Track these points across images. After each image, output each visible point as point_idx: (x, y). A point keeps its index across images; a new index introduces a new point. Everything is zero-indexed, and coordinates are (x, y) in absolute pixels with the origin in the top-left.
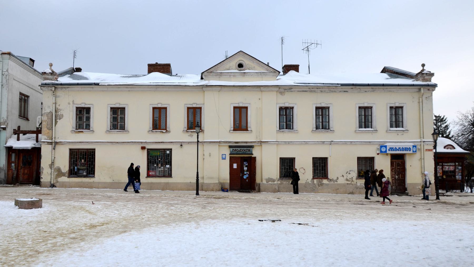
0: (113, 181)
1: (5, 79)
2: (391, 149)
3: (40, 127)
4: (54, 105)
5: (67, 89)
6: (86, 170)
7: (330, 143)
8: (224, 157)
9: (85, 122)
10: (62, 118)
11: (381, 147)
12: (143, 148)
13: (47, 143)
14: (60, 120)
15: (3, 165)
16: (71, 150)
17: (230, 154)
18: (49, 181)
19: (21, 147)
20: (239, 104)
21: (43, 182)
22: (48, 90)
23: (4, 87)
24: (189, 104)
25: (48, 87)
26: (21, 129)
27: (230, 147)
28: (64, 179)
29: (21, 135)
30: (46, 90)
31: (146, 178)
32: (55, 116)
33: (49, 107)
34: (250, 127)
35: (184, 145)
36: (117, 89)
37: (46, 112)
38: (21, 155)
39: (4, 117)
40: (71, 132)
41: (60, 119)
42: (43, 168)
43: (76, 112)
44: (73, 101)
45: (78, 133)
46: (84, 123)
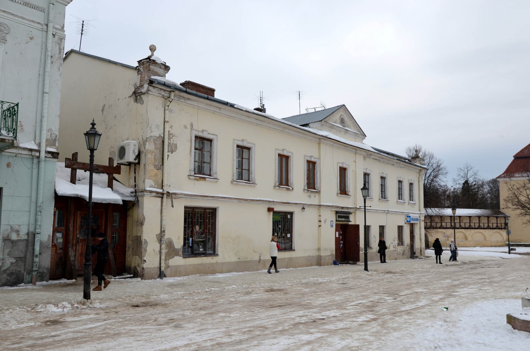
5: (187, 102)
10: (176, 151)
13: (155, 194)
14: (172, 153)
15: (47, 237)
18: (156, 266)
19: (105, 200)
21: (147, 268)
22: (159, 95)
23: (54, 63)
25: (161, 89)
26: (79, 160)
28: (178, 261)
30: (155, 94)
36: (246, 119)
37: (153, 134)
38: (78, 214)
39: (54, 129)
42: (146, 242)
44: (192, 125)
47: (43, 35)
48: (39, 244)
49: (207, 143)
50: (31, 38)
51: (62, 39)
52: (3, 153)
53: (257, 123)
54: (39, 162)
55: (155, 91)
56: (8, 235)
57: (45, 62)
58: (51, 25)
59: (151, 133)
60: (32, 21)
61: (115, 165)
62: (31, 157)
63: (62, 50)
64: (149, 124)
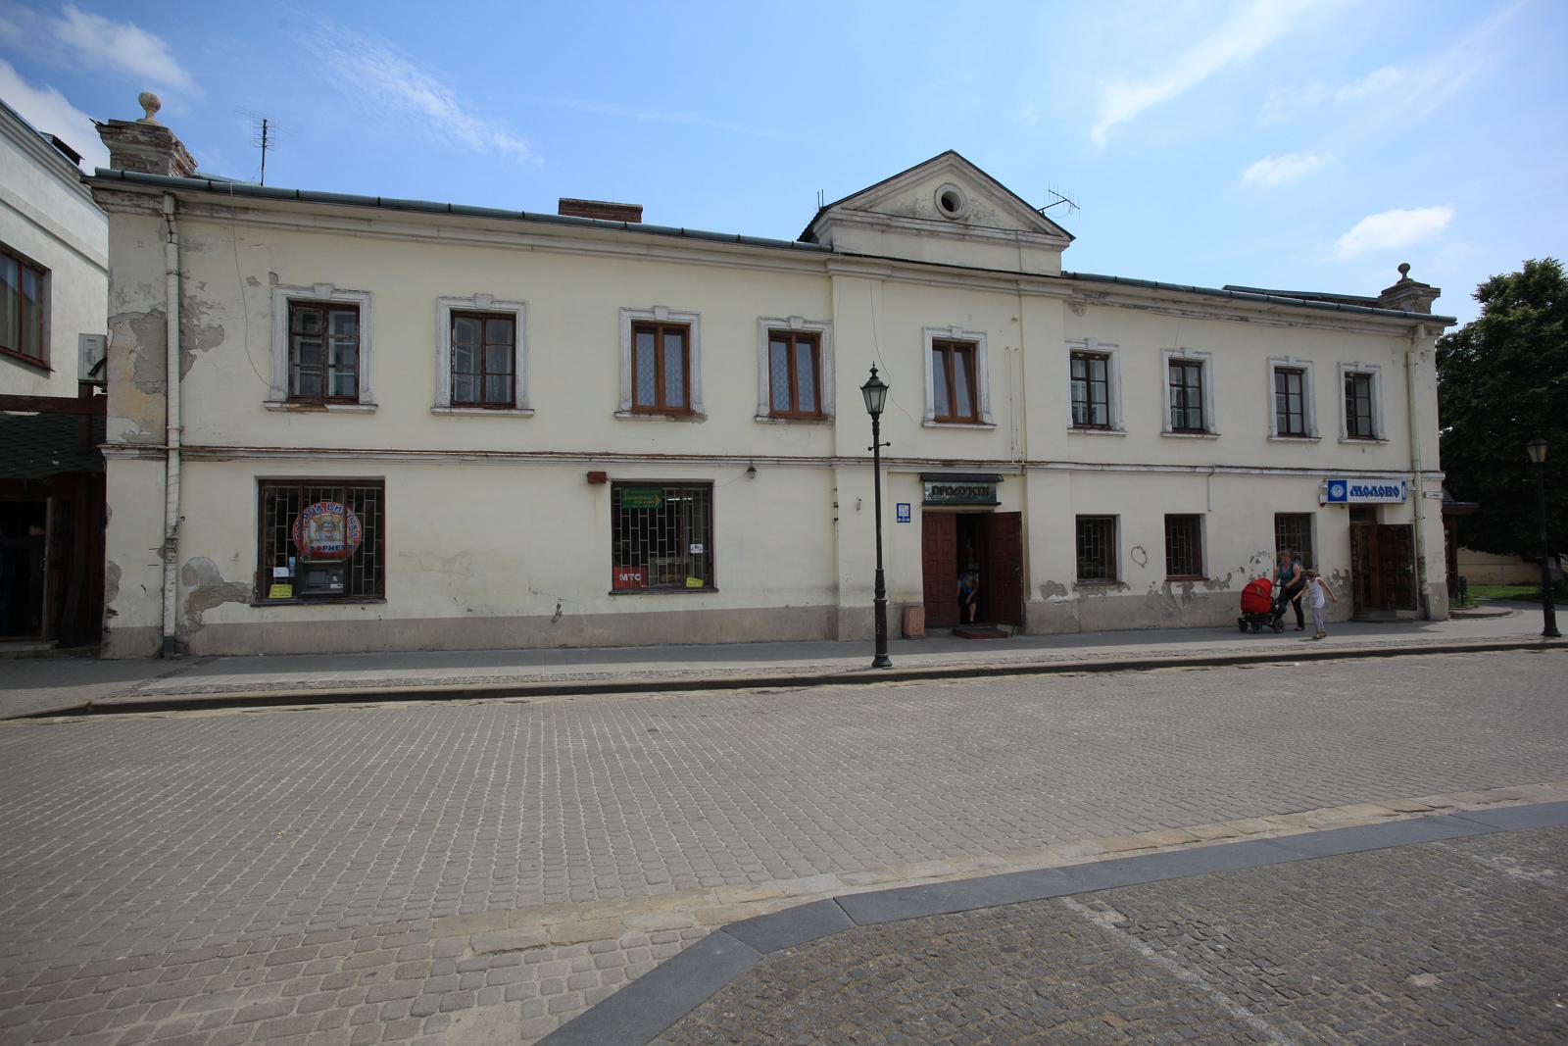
0: (470, 615)
2: (1357, 490)
3: (100, 377)
4: (173, 280)
6: (341, 572)
7: (1210, 470)
8: (903, 512)
9: (333, 366)
11: (1331, 484)
12: (596, 479)
13: (137, 452)
16: (262, 483)
17: (925, 503)
20: (951, 331)
21: (114, 628)
22: (140, 210)
24: (778, 319)
25: (139, 195)
27: (924, 478)
31: (612, 598)
32: (181, 331)
33: (146, 289)
34: (988, 412)
35: (760, 472)
40: (267, 405)
41: (206, 346)
42: (116, 569)
43: (291, 320)
44: (274, 276)
45: (301, 412)
46: (326, 371)
49: (672, 343)
53: (531, 242)
55: (120, 202)
59: (122, 305)
64: (115, 285)
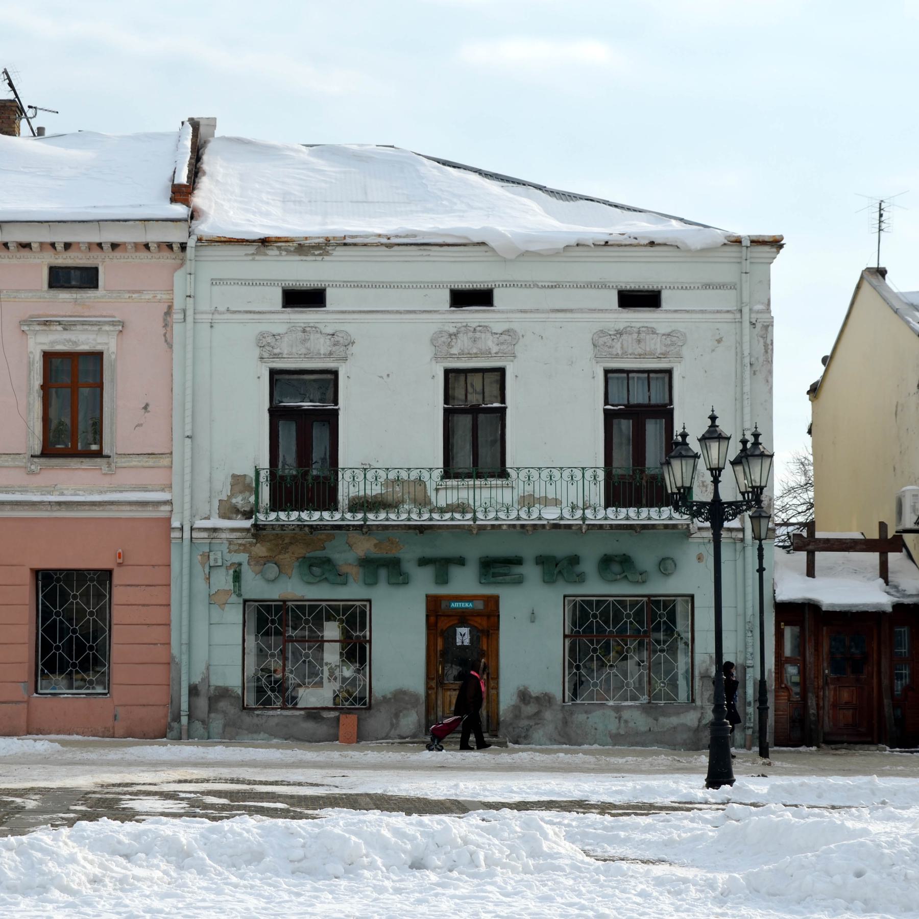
1: (762, 340)
19: (857, 606)
23: (757, 373)
29: (819, 556)
38: (824, 633)
47: (736, 329)
48: (752, 683)
50: (719, 341)
51: (768, 326)
52: (690, 540)
54: (744, 547)
56: (708, 669)
57: (742, 377)
58: (746, 310)
60: (718, 312)
61: (890, 536)
62: (732, 541)
63: (770, 347)
